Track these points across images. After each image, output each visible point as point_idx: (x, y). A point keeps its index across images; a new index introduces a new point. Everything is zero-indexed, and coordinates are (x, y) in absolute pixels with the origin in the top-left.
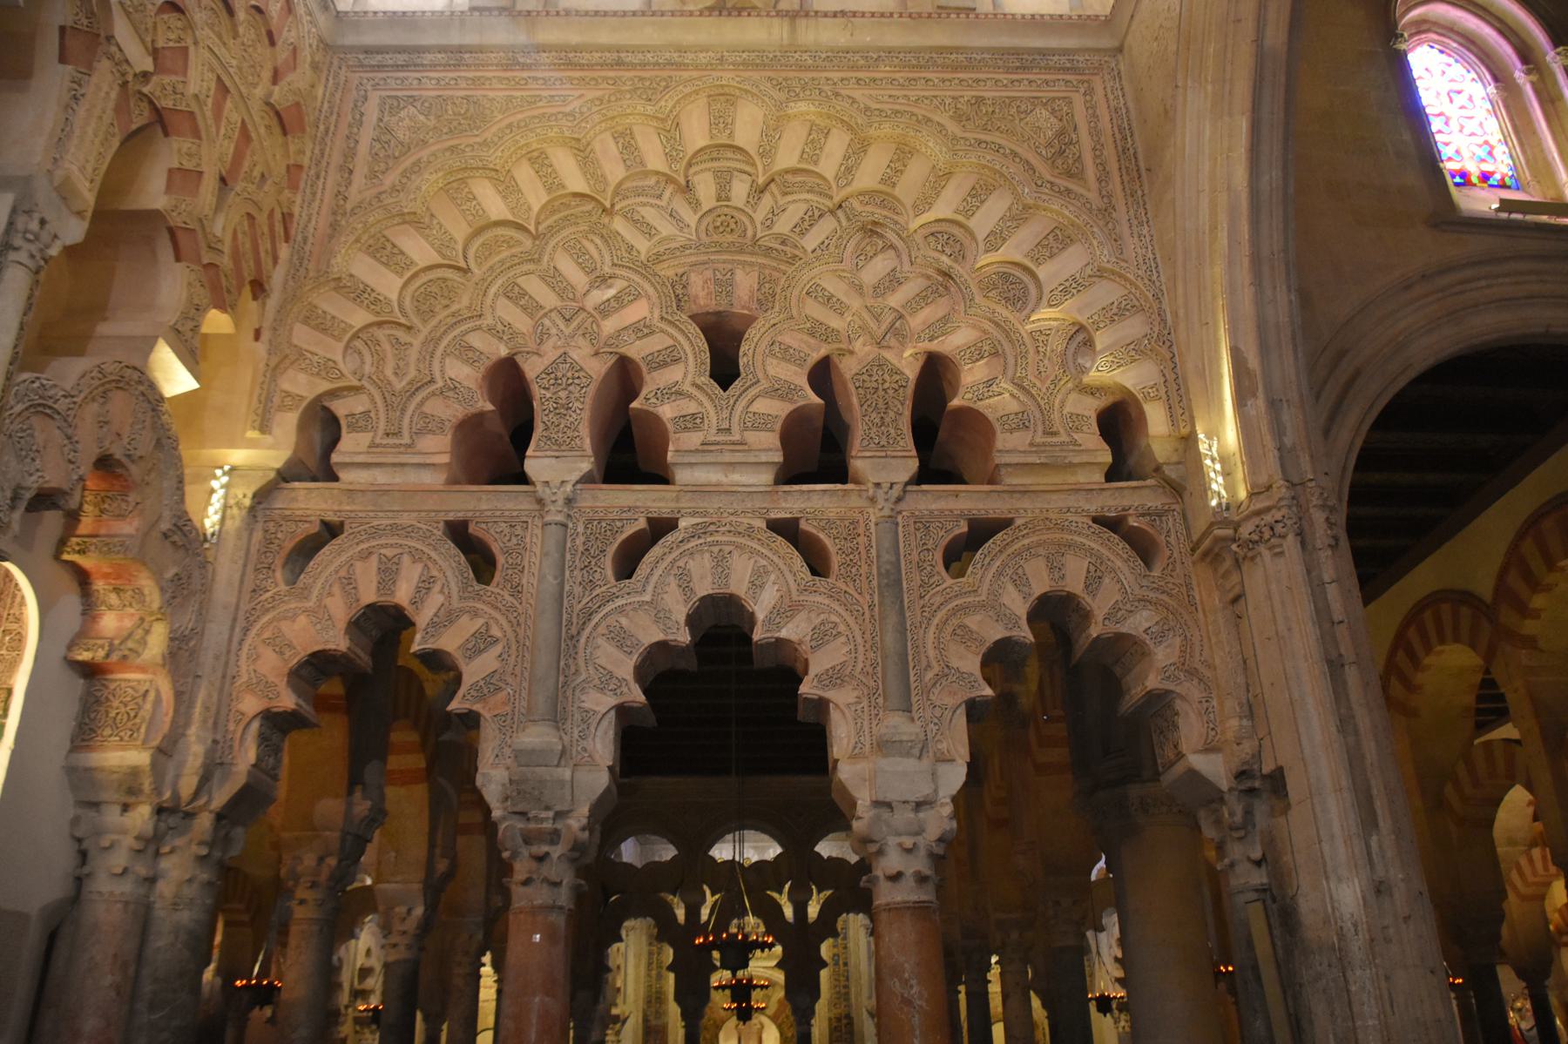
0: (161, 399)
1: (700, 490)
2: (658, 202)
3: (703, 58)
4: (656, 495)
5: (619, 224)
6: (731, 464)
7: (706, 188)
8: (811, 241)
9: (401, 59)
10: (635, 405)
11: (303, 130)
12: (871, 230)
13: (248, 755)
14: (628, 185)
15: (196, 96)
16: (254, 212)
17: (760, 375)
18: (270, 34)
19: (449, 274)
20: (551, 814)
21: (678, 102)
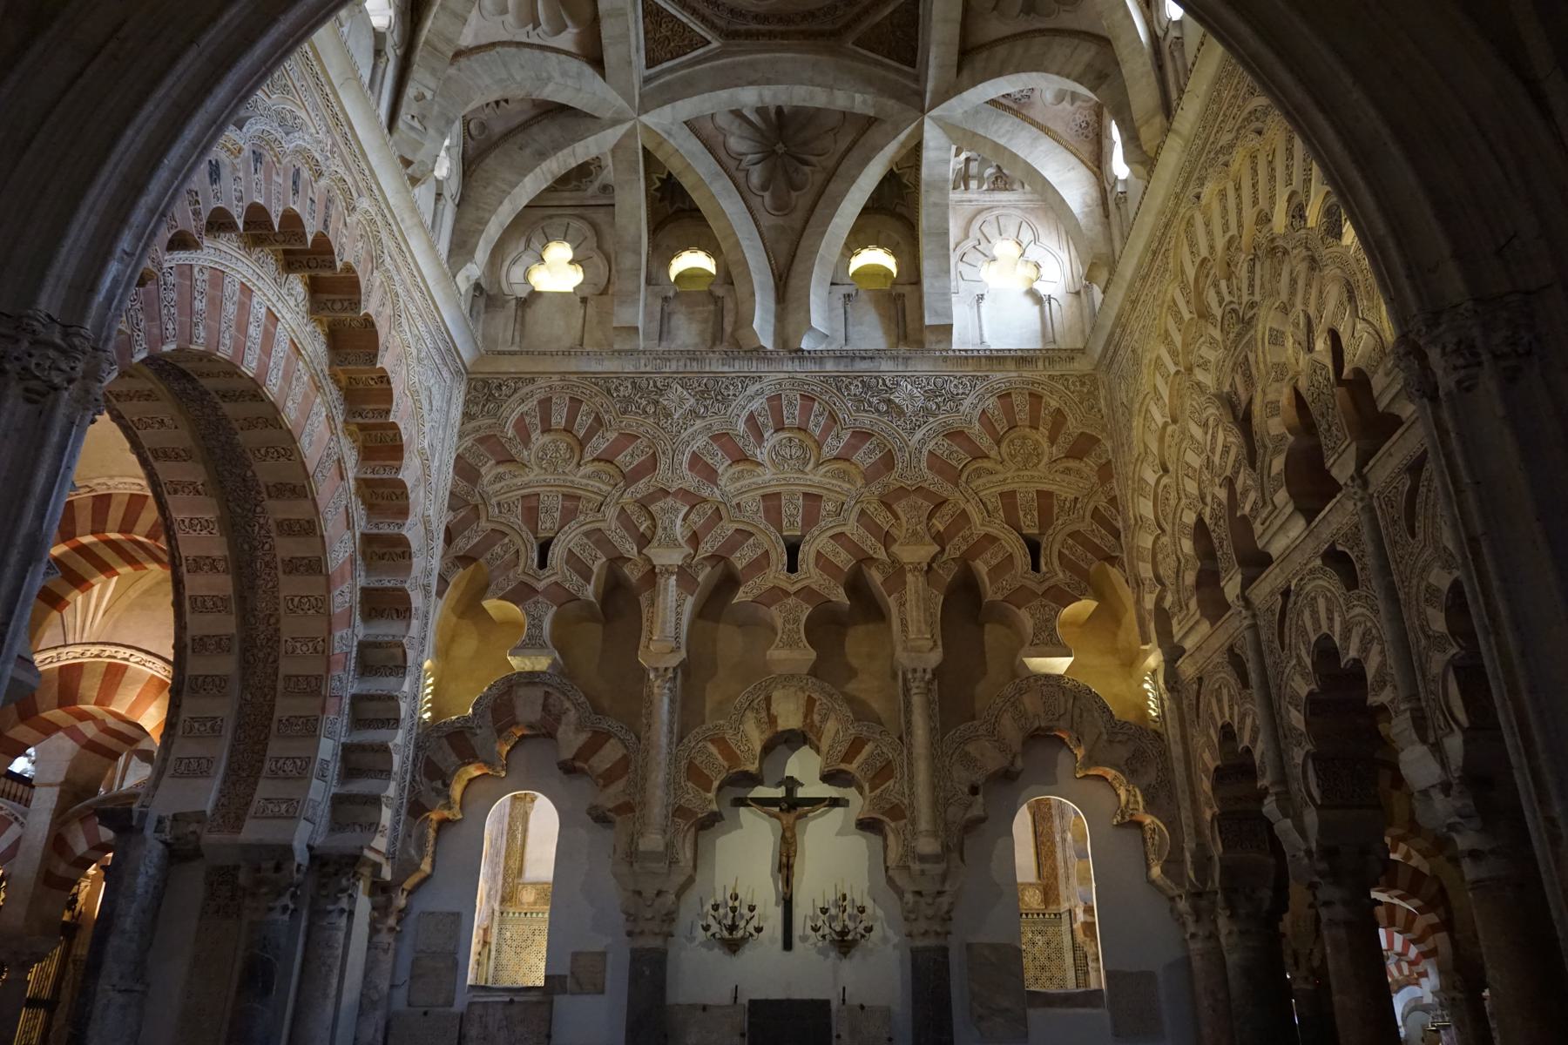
0: (1060, 676)
1: (1286, 555)
2: (1203, 339)
4: (1272, 575)
5: (1199, 375)
6: (1281, 527)
8: (1257, 298)
9: (1112, 348)
10: (1238, 514)
11: (1099, 440)
12: (1272, 251)
13: (1217, 849)
14: (1189, 340)
15: (982, 525)
16: (1075, 527)
17: (1267, 442)
18: (1031, 427)
19: (1165, 480)
20: (1302, 854)
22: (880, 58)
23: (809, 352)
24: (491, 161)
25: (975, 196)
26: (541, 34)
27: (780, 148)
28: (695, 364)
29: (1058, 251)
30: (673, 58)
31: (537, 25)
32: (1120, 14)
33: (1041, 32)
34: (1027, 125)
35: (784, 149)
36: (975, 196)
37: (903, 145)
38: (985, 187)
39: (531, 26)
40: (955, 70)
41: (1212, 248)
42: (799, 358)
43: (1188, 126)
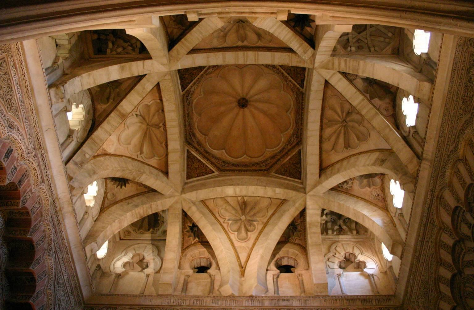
2: (464, 251)
3: (429, 197)
7: (465, 230)
21: (437, 217)
22: (285, 177)
23: (256, 297)
24: (113, 208)
25: (331, 237)
26: (143, 157)
27: (243, 218)
28: (198, 302)
29: (373, 257)
30: (198, 176)
31: (142, 153)
32: (388, 130)
33: (354, 155)
34: (351, 197)
35: (245, 218)
36: (331, 237)
37: (297, 209)
38: (335, 233)
39: (139, 153)
40: (318, 175)
41: (458, 199)
42: (251, 300)
43: (430, 154)
